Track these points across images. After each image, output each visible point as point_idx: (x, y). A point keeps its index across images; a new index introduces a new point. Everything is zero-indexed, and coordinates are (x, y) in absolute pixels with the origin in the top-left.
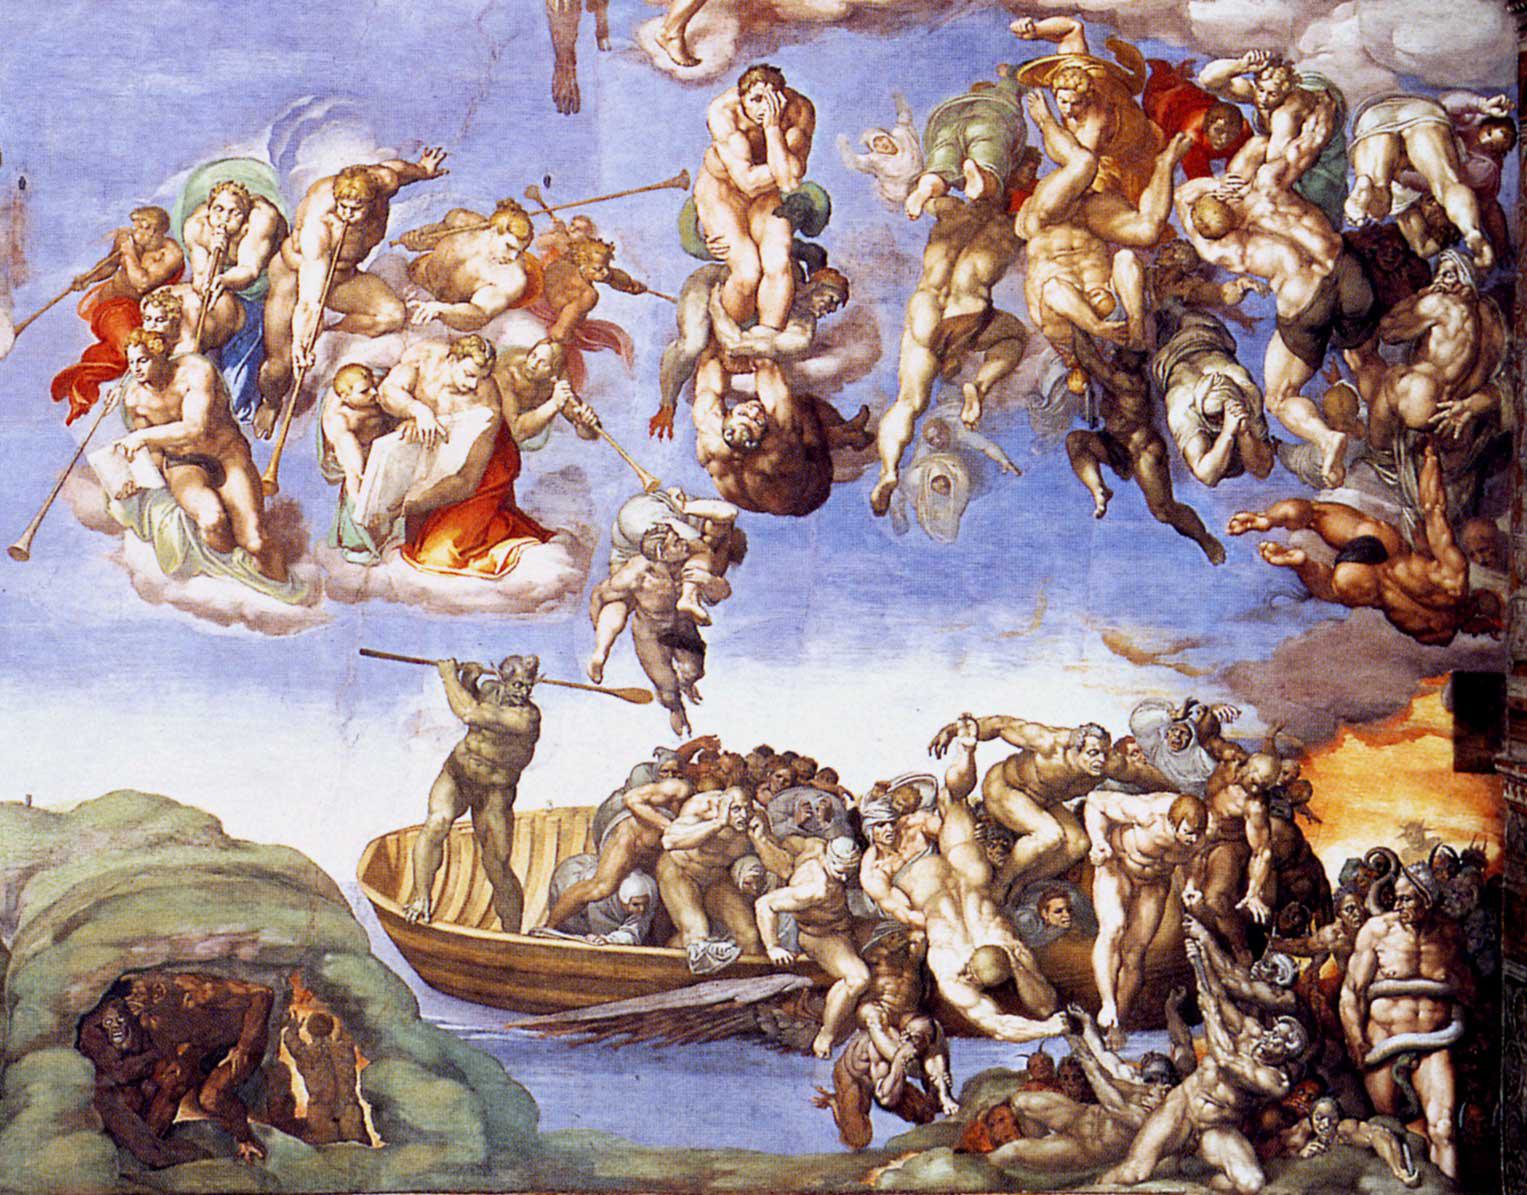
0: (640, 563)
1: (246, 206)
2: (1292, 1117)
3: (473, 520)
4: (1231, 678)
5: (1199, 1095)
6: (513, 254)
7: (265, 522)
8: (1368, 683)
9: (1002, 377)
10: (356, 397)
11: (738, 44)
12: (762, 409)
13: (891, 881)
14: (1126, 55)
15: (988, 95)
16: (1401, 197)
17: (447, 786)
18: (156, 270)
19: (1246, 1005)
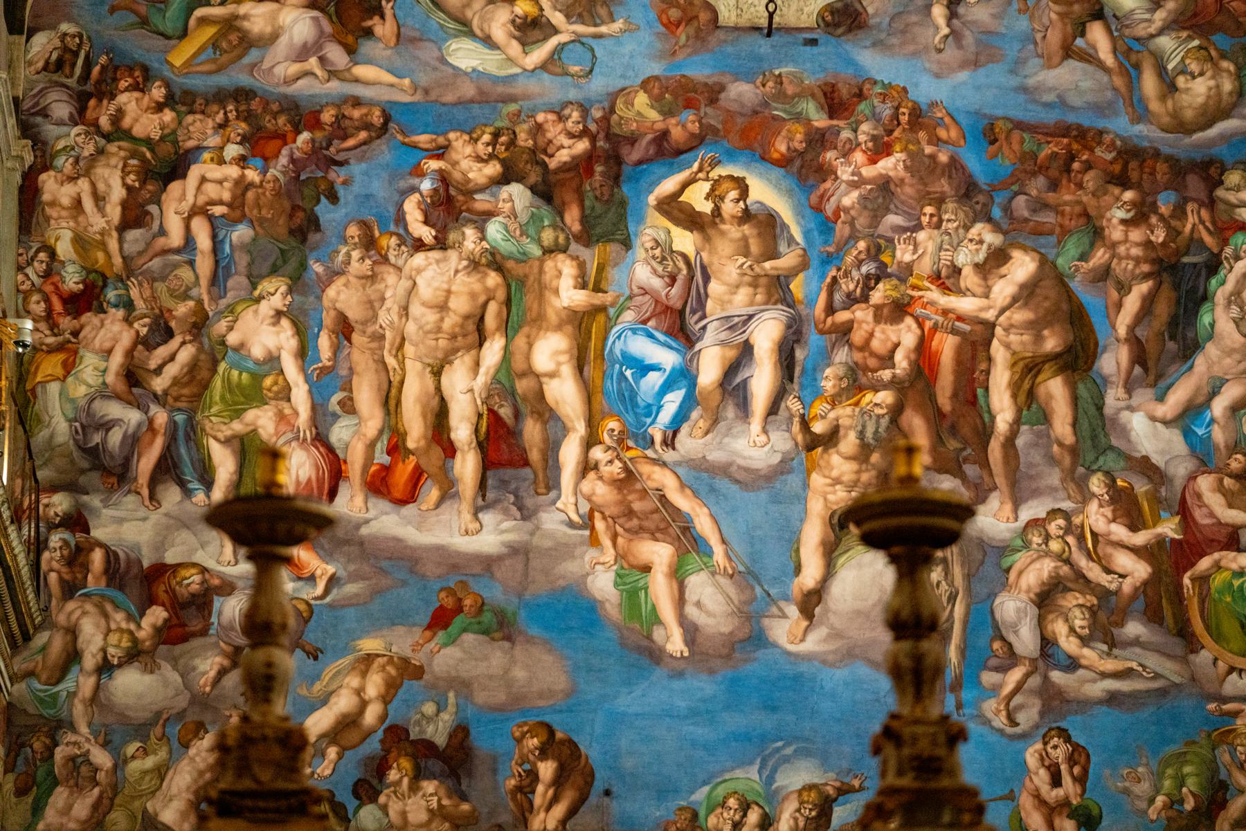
1: (745, 807)
11: (1042, 714)
15: (1195, 748)
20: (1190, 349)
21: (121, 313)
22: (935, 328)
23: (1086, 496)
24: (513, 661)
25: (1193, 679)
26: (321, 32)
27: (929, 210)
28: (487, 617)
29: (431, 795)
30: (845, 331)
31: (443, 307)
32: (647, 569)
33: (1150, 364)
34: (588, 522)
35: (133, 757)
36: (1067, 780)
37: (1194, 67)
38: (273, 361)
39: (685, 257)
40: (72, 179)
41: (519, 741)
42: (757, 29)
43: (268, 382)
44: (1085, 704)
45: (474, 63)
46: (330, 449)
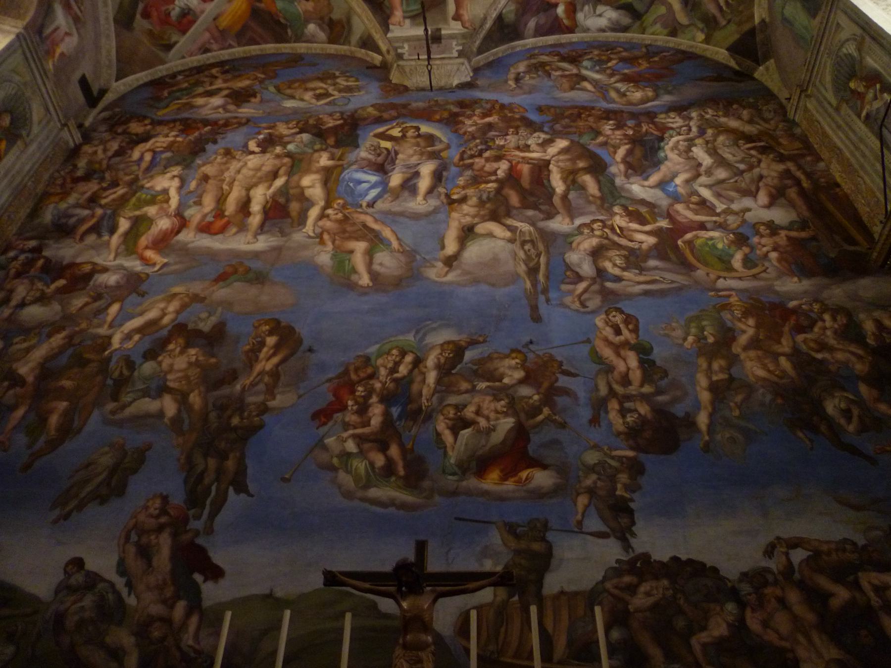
0: (594, 477)
1: (403, 354)
6: (519, 366)
7: (406, 466)
10: (451, 415)
11: (603, 301)
12: (640, 414)
13: (765, 624)
18: (362, 375)
20: (657, 164)
22: (519, 162)
23: (613, 214)
25: (696, 282)
27: (511, 130)
28: (251, 275)
29: (193, 355)
31: (258, 169)
32: (352, 252)
34: (320, 236)
35: (16, 343)
36: (625, 332)
38: (165, 191)
41: (256, 328)
43: (159, 198)
44: (630, 296)
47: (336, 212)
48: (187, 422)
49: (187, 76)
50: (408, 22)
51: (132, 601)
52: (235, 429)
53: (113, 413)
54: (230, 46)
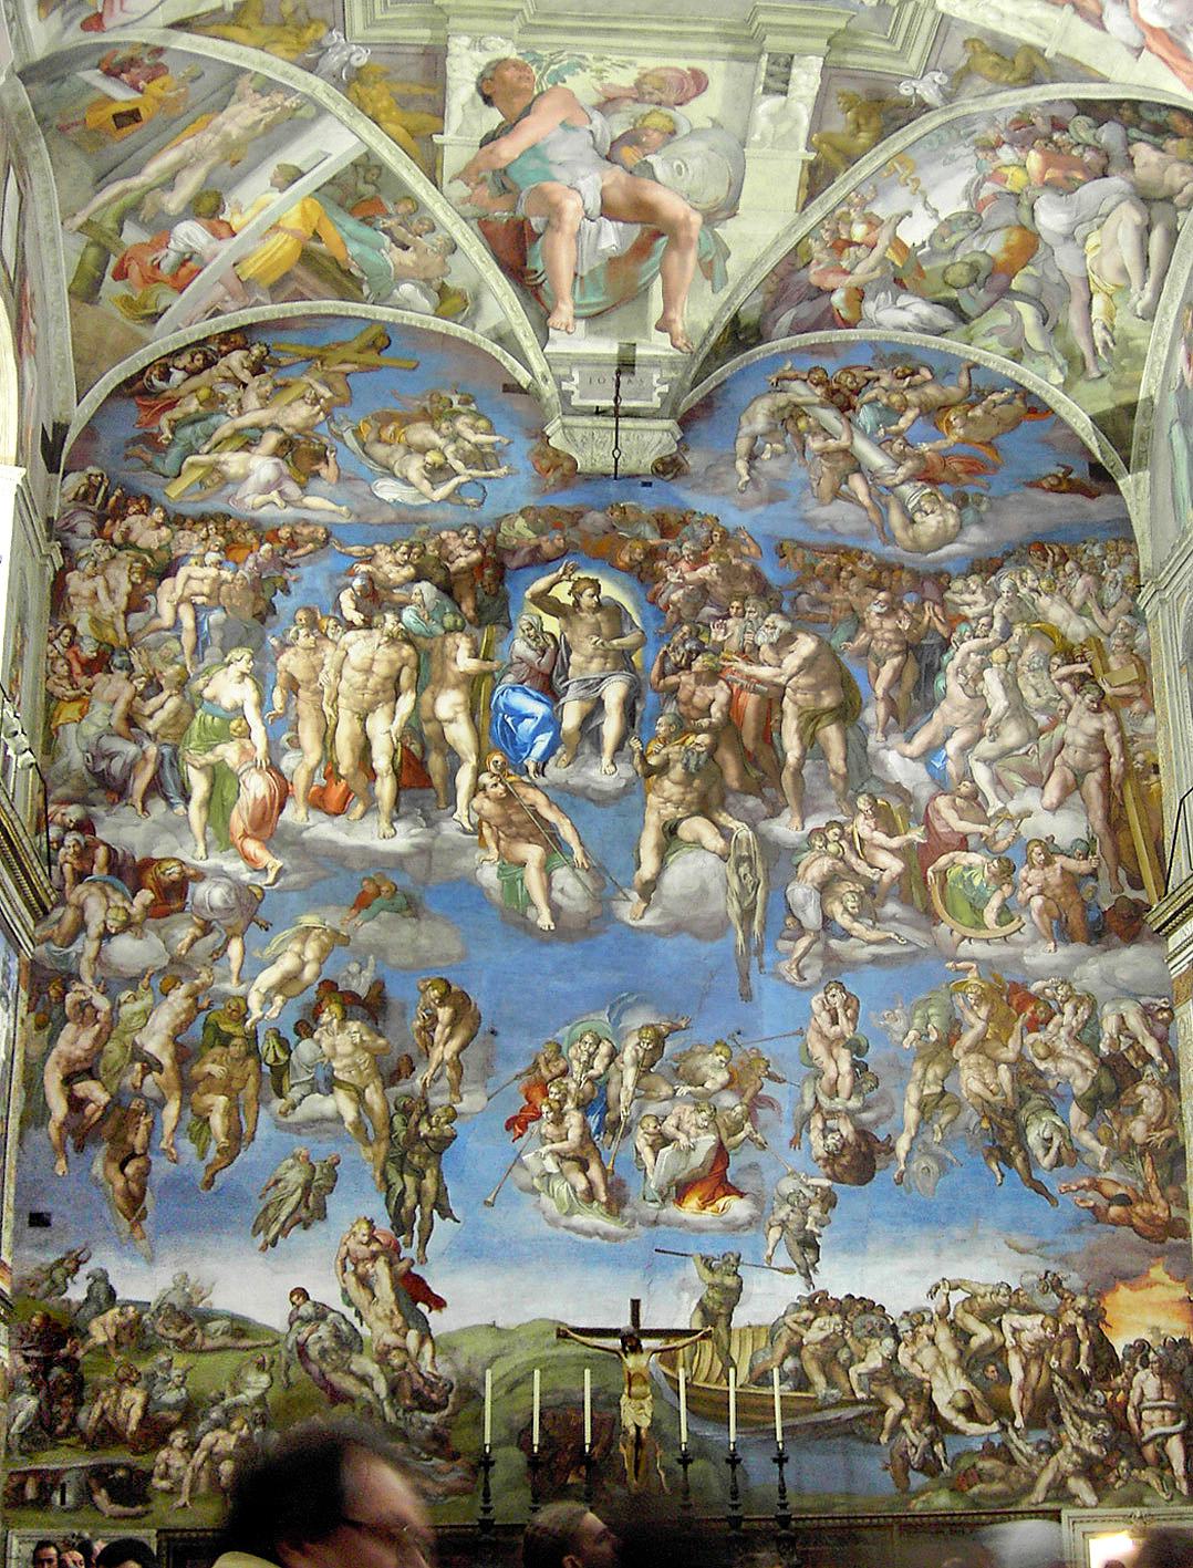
0: (788, 1208)
1: (598, 1042)
2: (1109, 1468)
3: (706, 1189)
4: (1064, 1260)
5: (1065, 1460)
7: (608, 1189)
8: (1128, 1261)
9: (952, 1121)
10: (651, 1130)
11: (823, 972)
13: (913, 1359)
14: (997, 979)
16: (1125, 1043)
17: (699, 1315)
18: (555, 1071)
19: (1083, 1415)
20: (931, 705)
21: (124, 673)
22: (741, 688)
23: (856, 811)
24: (419, 932)
26: (281, 474)
27: (736, 604)
30: (673, 691)
31: (368, 671)
33: (901, 716)
34: (478, 829)
36: (842, 1019)
37: (927, 507)
38: (239, 710)
39: (552, 635)
40: (91, 577)
41: (423, 992)
42: (607, 475)
43: (234, 724)
45: (395, 496)
46: (281, 774)
47: (493, 781)
48: (370, 1131)
49: (192, 373)
50: (581, 324)
51: (364, 1331)
52: (426, 1138)
53: (285, 1114)
54: (258, 303)
